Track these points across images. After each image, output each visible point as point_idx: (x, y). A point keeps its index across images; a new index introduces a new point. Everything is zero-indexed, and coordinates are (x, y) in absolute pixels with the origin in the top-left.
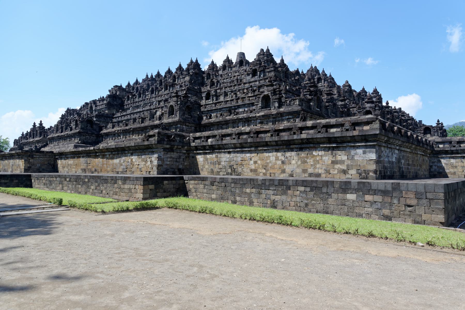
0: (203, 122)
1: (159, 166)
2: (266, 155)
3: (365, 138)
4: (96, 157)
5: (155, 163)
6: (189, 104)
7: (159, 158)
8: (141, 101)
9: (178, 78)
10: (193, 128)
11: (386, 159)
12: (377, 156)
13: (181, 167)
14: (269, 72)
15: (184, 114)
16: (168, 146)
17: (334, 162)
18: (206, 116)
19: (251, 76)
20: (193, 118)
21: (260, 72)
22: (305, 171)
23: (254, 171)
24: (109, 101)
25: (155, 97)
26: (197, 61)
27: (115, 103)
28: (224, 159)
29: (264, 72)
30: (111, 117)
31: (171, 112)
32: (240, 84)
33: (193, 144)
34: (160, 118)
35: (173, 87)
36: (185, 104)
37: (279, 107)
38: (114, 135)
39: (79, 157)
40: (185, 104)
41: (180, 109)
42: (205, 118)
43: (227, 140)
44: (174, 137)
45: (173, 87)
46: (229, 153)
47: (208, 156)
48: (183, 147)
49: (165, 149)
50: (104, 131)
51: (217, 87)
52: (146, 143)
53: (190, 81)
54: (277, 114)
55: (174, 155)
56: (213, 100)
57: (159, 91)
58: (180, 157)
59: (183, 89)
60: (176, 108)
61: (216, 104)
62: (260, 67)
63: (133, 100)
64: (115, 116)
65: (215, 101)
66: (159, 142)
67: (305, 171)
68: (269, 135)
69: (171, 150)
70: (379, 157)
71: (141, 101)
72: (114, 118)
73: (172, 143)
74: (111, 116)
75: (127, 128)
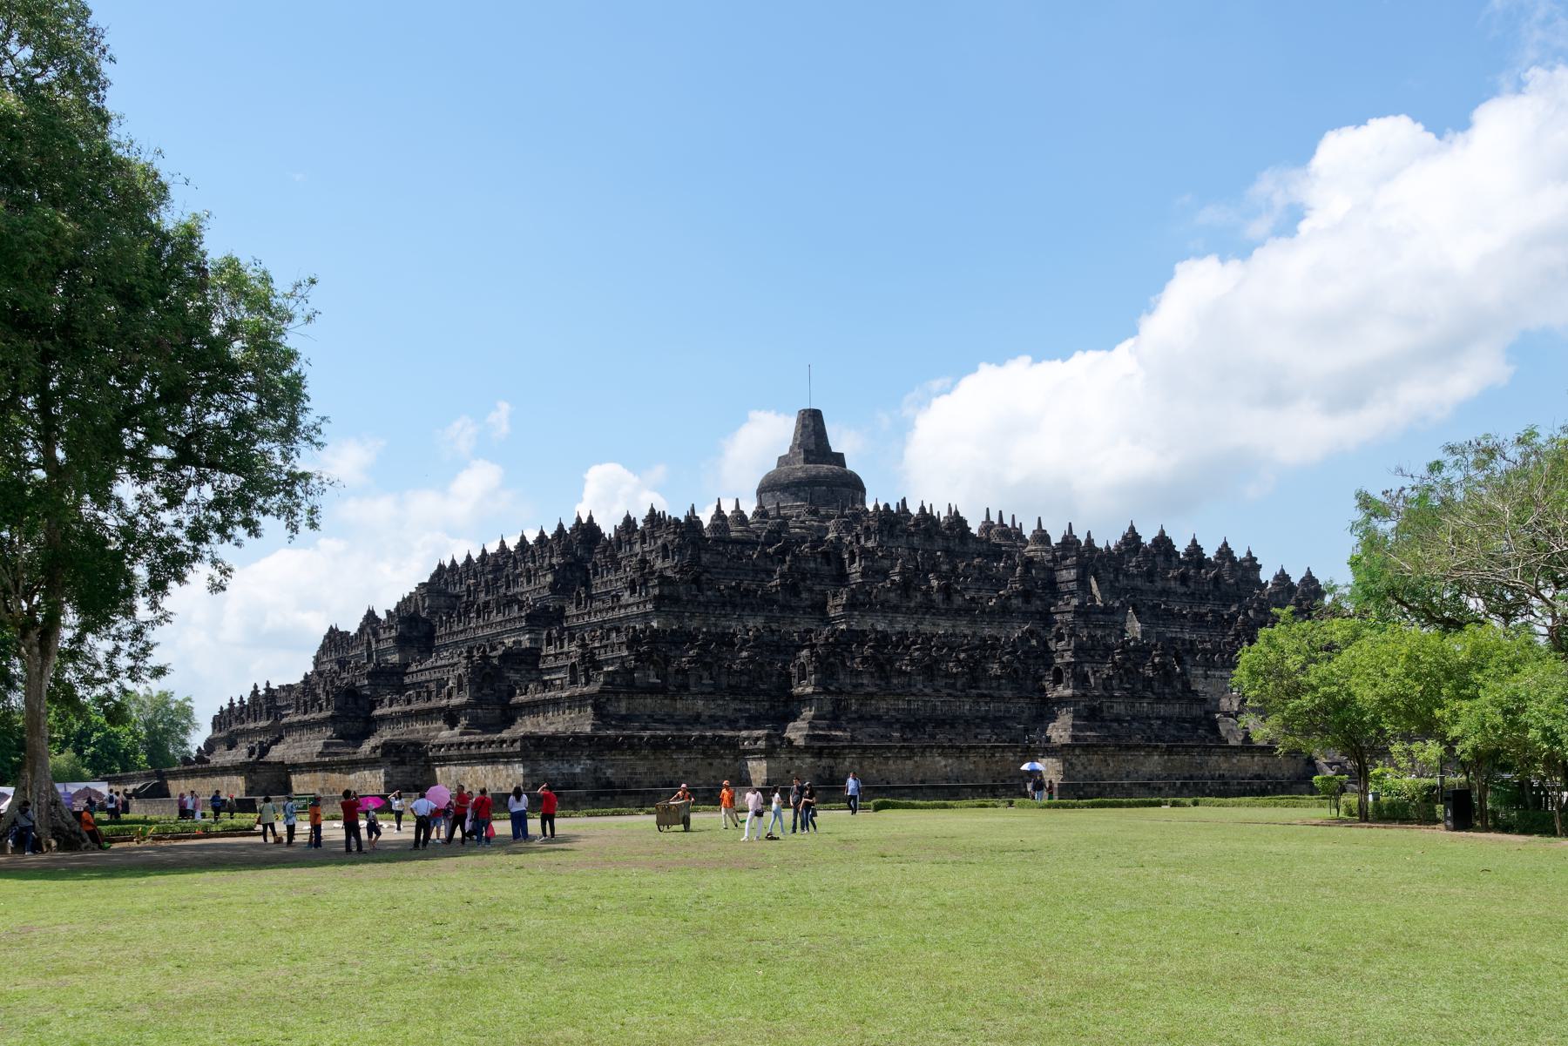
0: (514, 700)
1: (386, 783)
2: (477, 768)
3: (516, 755)
4: (333, 771)
5: (383, 780)
6: (488, 670)
7: (386, 774)
8: (461, 632)
9: (535, 575)
10: (498, 712)
11: (555, 772)
12: (527, 770)
13: (418, 782)
14: (653, 587)
15: (480, 689)
16: (397, 759)
17: (508, 776)
18: (521, 689)
19: (629, 592)
20: (497, 694)
21: (641, 585)
22: (495, 785)
23: (470, 785)
24: (401, 633)
25: (482, 627)
26: (591, 518)
27: (415, 634)
28: (453, 773)
29: (647, 587)
30: (400, 671)
31: (460, 687)
32: (613, 609)
33: (430, 754)
34: (450, 696)
35: (509, 607)
36: (481, 670)
37: (587, 684)
38: (392, 719)
39: (315, 771)
40: (481, 670)
41: (470, 680)
42: (518, 691)
43: (453, 752)
44: (405, 747)
45: (509, 607)
46: (456, 765)
47: (443, 769)
48: (419, 757)
49: (393, 763)
50: (378, 712)
51: (586, 607)
52: (373, 756)
53: (552, 587)
54: (580, 695)
55: (408, 769)
56: (556, 647)
57: (489, 613)
58: (415, 771)
59: (523, 614)
60: (465, 680)
61: (556, 656)
62: (642, 575)
63: (451, 627)
64: (408, 671)
65: (558, 651)
66: (383, 755)
67: (495, 785)
68: (473, 747)
69: (402, 762)
70: (533, 770)
71: (461, 632)
72: (407, 674)
73: (402, 755)
74: (400, 670)
75: (408, 708)
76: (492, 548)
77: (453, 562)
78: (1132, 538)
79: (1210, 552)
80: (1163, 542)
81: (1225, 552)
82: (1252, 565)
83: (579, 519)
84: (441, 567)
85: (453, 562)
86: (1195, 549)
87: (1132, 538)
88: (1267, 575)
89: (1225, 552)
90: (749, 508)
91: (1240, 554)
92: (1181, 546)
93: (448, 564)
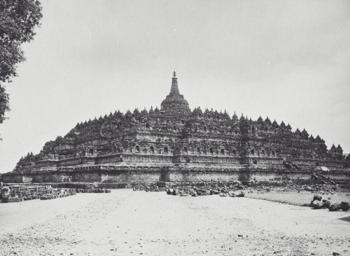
76: (92, 119)
77: (82, 123)
78: (260, 119)
79: (279, 123)
80: (268, 120)
81: (283, 124)
82: (289, 127)
83: (116, 111)
84: (78, 124)
85: (82, 123)
86: (275, 122)
87: (260, 119)
88: (293, 130)
89: (283, 124)
90: (159, 108)
91: (286, 125)
92: (272, 122)
93: (80, 123)
